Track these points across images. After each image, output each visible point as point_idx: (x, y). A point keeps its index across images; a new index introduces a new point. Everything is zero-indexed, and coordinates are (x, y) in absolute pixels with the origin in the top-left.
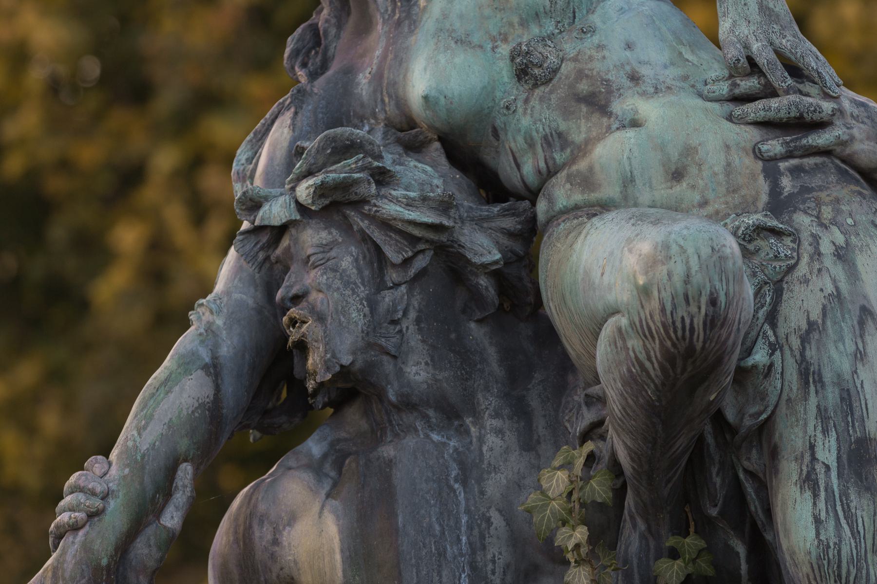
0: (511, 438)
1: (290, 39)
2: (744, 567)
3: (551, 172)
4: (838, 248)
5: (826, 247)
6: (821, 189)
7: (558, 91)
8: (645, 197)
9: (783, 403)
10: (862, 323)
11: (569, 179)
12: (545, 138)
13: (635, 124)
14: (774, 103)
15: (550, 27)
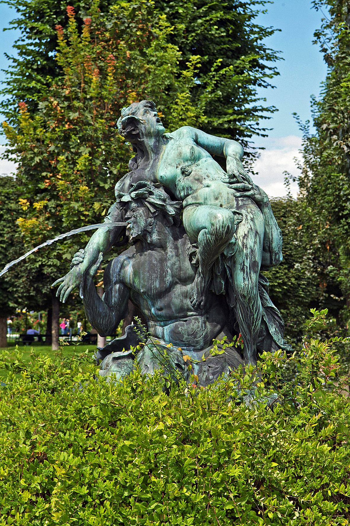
0: (174, 253)
5: (249, 218)
7: (191, 178)
8: (209, 203)
10: (256, 235)
13: (208, 186)
14: (239, 185)
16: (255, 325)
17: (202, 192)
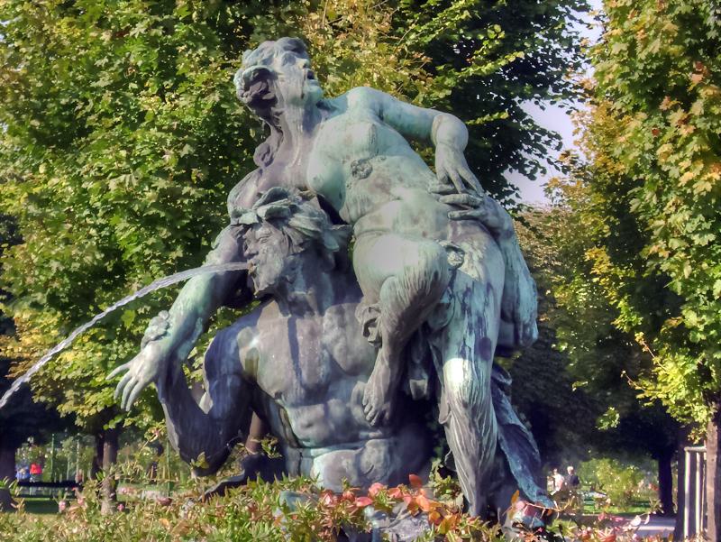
5: (475, 258)
6: (473, 233)
9: (453, 321)
10: (488, 290)
11: (370, 218)
13: (399, 199)
16: (485, 457)
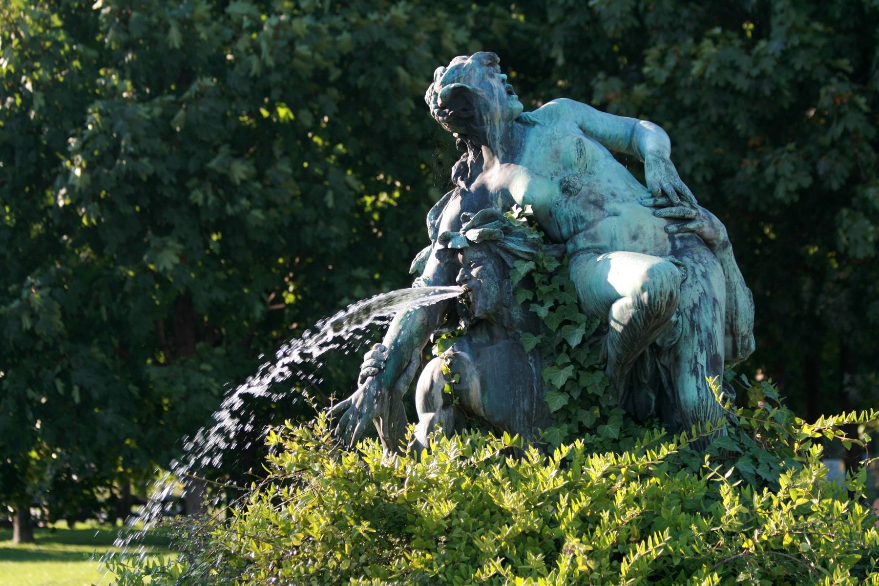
1: (453, 168)
2: (653, 404)
3: (576, 232)
4: (703, 273)
5: (698, 272)
6: (692, 247)
9: (683, 338)
10: (714, 305)
11: (585, 236)
12: (574, 218)
13: (616, 215)
14: (674, 209)
15: (576, 170)
17: (606, 227)
